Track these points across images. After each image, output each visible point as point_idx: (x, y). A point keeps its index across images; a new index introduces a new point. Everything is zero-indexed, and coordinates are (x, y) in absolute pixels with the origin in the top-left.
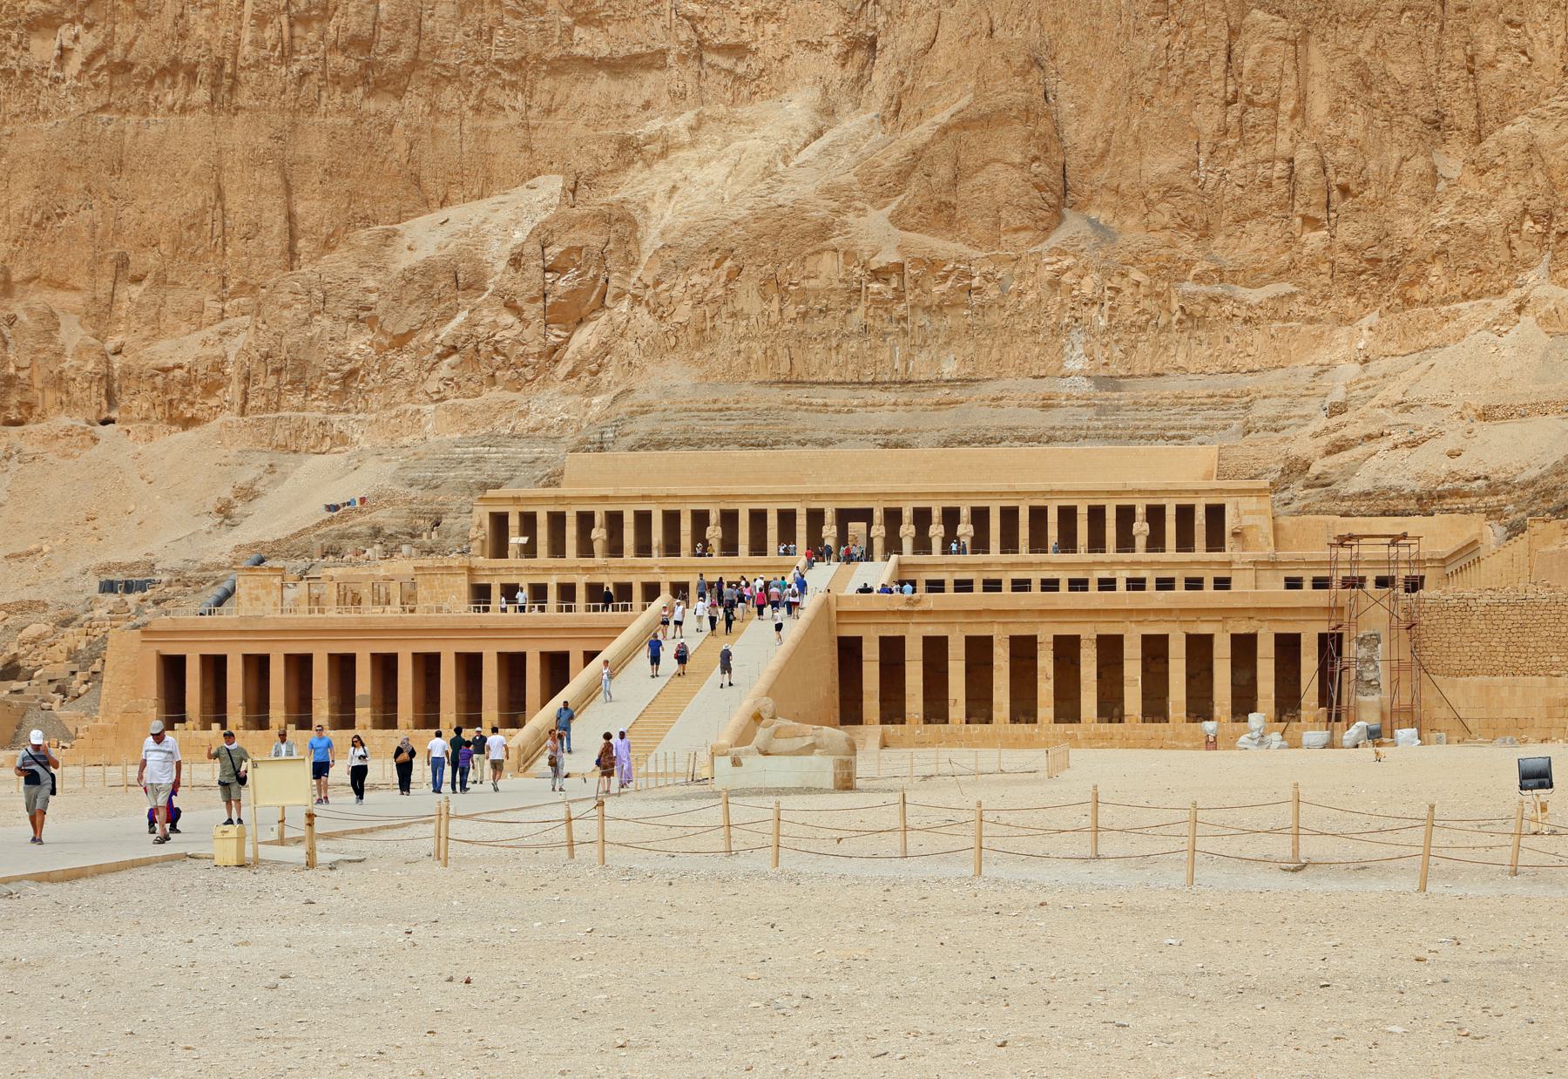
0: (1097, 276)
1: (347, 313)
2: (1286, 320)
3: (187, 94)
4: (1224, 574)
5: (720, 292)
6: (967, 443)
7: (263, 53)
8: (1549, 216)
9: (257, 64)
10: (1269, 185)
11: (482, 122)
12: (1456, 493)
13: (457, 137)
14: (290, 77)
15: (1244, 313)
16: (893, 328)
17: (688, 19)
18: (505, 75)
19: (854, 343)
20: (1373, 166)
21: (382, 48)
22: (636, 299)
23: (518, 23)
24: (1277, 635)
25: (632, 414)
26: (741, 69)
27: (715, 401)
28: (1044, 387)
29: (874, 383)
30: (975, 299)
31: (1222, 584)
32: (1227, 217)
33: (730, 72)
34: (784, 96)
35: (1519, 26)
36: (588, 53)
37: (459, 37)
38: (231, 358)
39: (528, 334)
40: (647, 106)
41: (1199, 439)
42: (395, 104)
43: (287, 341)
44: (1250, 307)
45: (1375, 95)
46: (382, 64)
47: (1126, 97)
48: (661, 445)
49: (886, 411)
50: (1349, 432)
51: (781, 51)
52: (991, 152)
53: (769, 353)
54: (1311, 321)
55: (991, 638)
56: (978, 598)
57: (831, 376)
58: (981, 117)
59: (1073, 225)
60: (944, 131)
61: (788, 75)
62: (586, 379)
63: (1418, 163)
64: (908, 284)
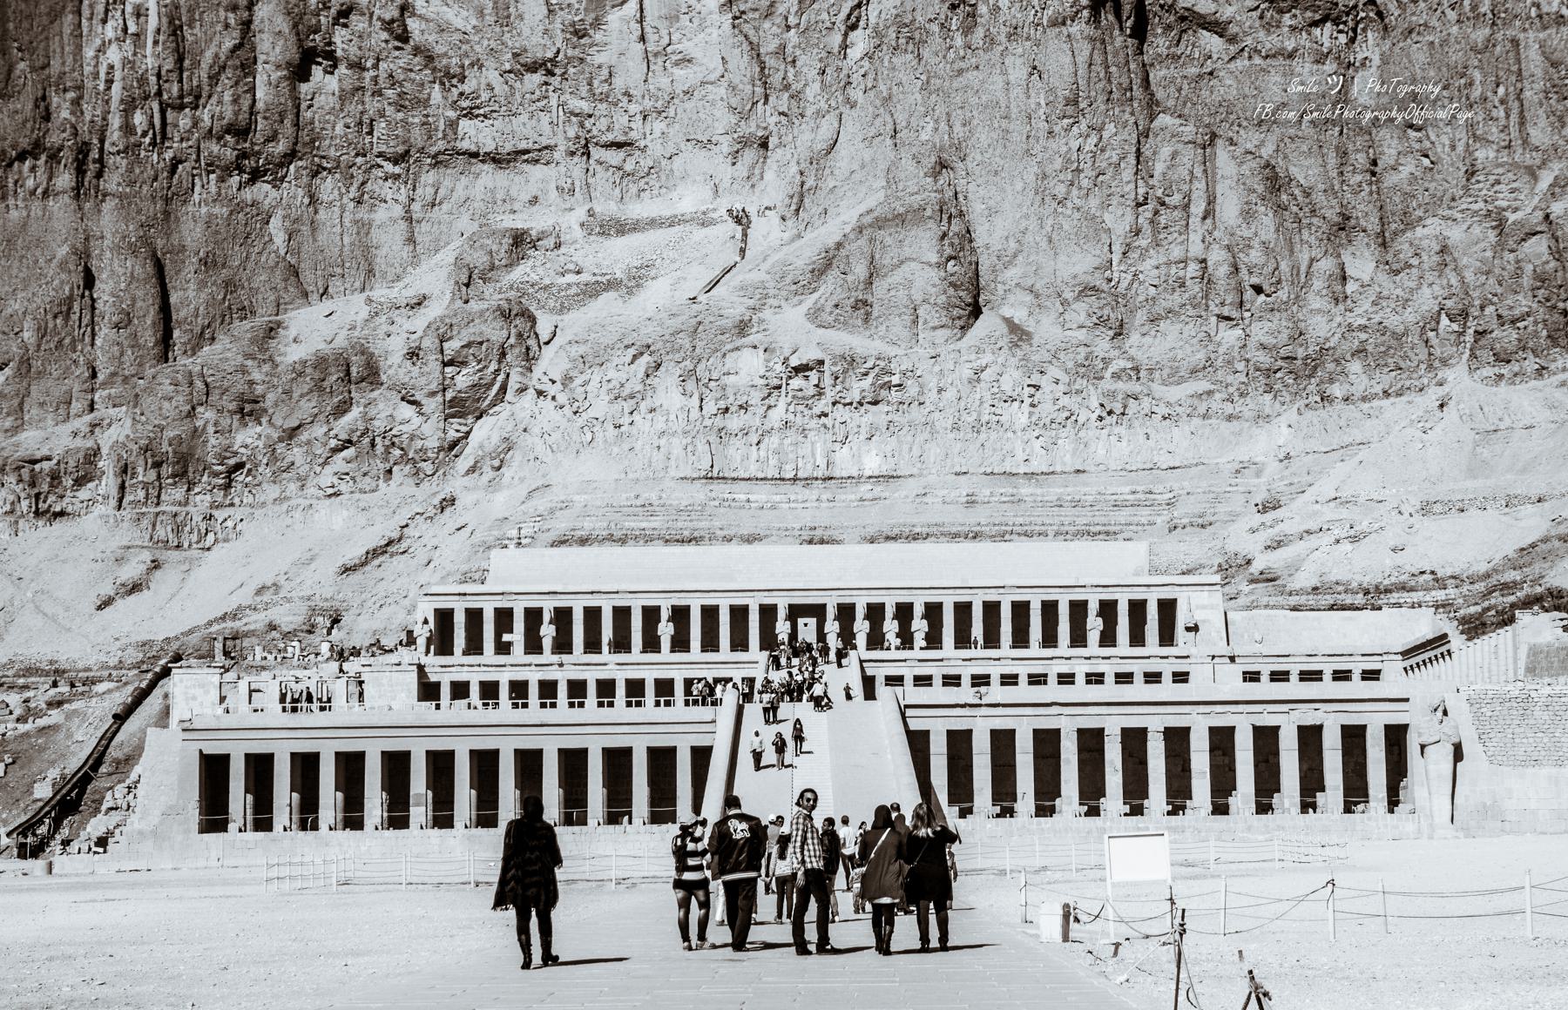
1: (233, 406)
2: (1205, 417)
3: (50, 179)
4: (1181, 667)
5: (640, 387)
6: (894, 539)
7: (132, 140)
8: (1464, 314)
9: (125, 151)
10: (1183, 285)
11: (362, 213)
12: (1403, 588)
13: (338, 229)
14: (162, 164)
15: (1162, 410)
16: (814, 423)
17: (576, 115)
18: (389, 167)
19: (773, 441)
20: (1284, 266)
21: (259, 138)
22: (540, 393)
23: (400, 115)
24: (1343, 727)
25: (552, 511)
26: (629, 167)
27: (637, 497)
28: (965, 486)
29: (795, 479)
30: (894, 395)
31: (1181, 677)
32: (1141, 316)
33: (619, 169)
34: (674, 195)
36: (473, 148)
37: (339, 129)
38: (105, 451)
39: (428, 429)
40: (534, 201)
41: (1126, 535)
42: (274, 193)
43: (170, 433)
44: (1168, 404)
45: (1284, 197)
46: (259, 153)
47: (1039, 198)
48: (583, 542)
49: (809, 507)
50: (1291, 528)
51: (671, 150)
52: (907, 252)
53: (690, 448)
54: (1230, 418)
55: (1058, 731)
56: (1139, 690)
57: (753, 470)
59: (987, 323)
60: (860, 230)
61: (677, 173)
62: (489, 474)
63: (1326, 265)
64: (828, 380)
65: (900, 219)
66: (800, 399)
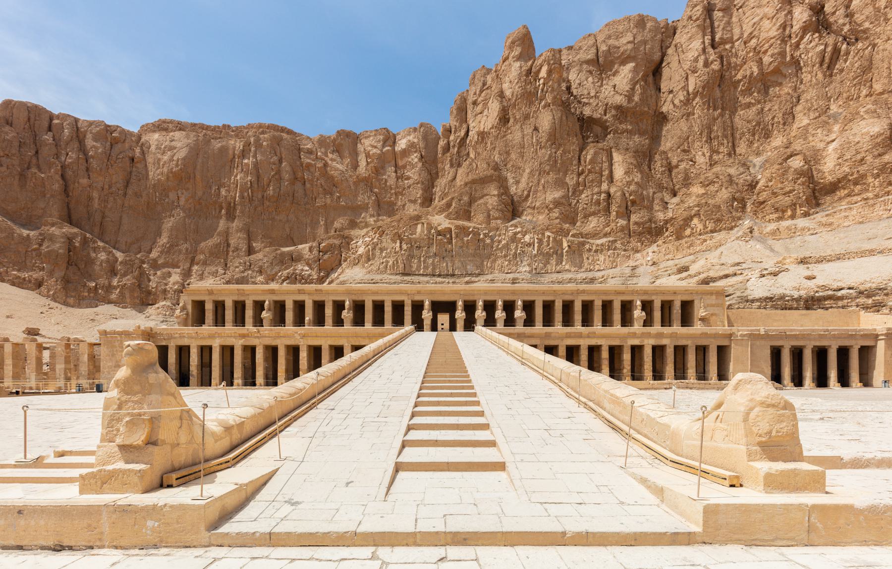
0: (532, 235)
2: (614, 249)
15: (594, 248)
28: (511, 276)
35: (688, 151)
44: (598, 245)
50: (712, 274)
52: (485, 192)
57: (421, 272)
58: (481, 179)
64: (454, 236)
65: (483, 181)
66: (440, 244)
